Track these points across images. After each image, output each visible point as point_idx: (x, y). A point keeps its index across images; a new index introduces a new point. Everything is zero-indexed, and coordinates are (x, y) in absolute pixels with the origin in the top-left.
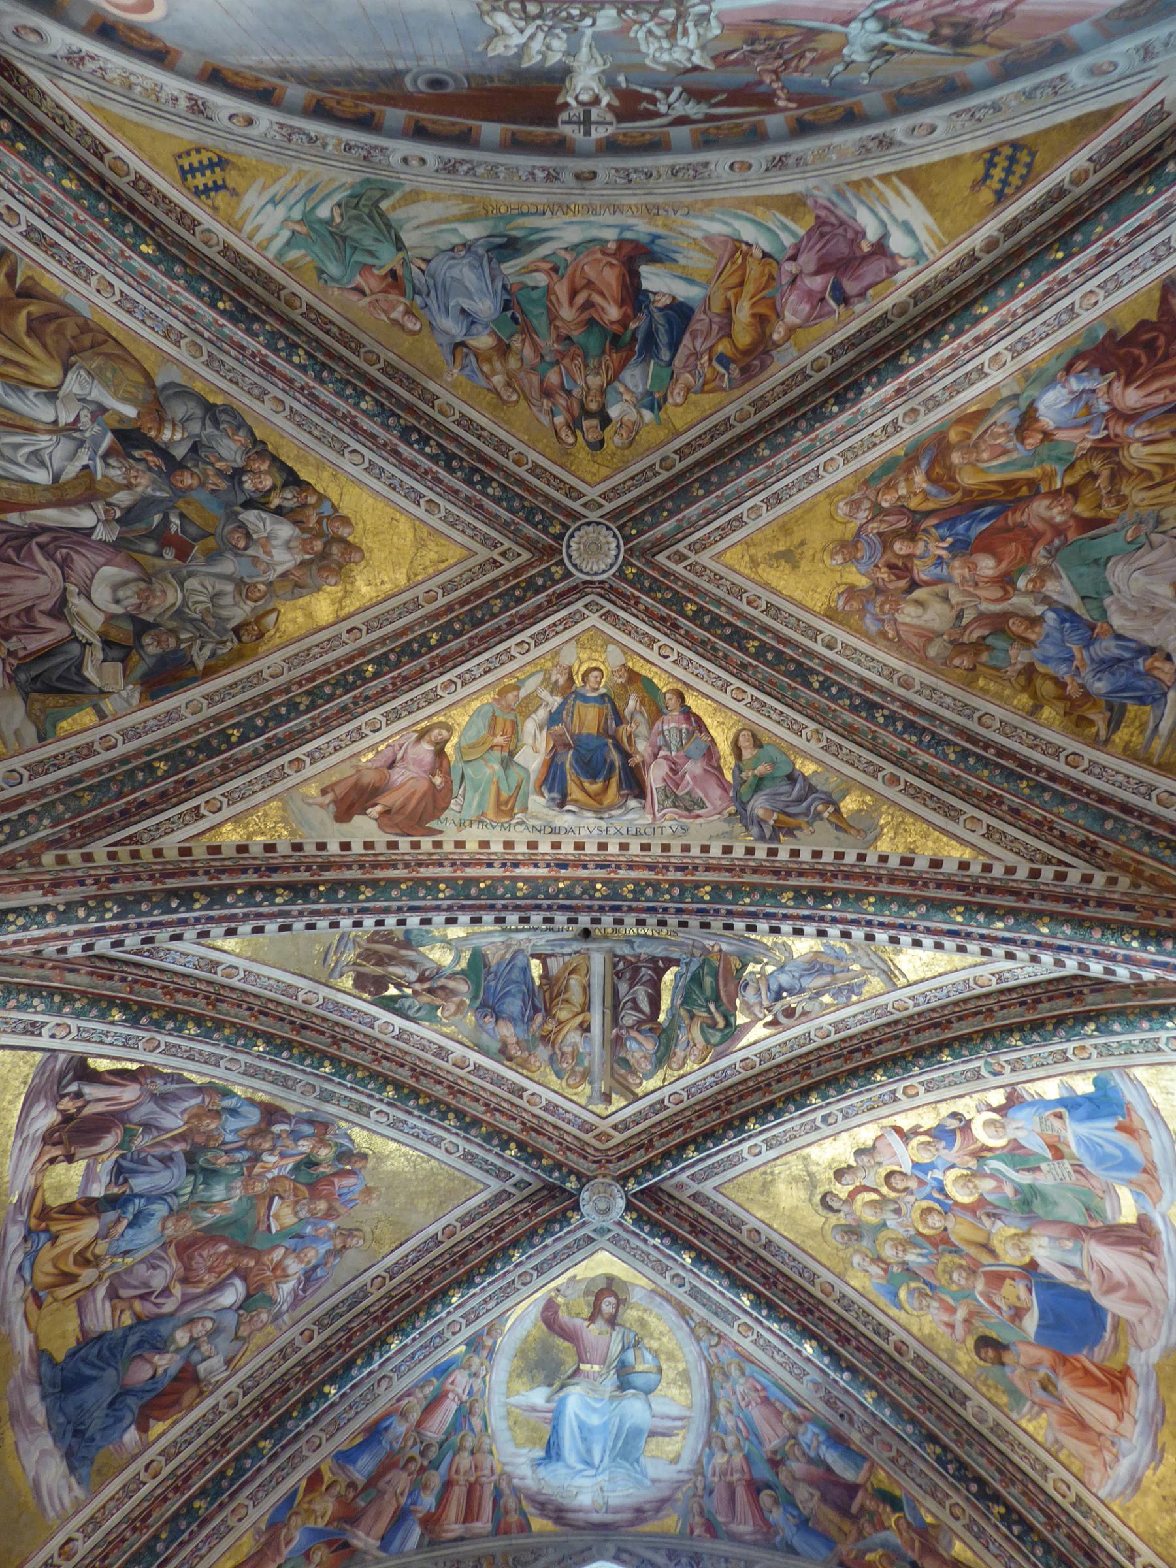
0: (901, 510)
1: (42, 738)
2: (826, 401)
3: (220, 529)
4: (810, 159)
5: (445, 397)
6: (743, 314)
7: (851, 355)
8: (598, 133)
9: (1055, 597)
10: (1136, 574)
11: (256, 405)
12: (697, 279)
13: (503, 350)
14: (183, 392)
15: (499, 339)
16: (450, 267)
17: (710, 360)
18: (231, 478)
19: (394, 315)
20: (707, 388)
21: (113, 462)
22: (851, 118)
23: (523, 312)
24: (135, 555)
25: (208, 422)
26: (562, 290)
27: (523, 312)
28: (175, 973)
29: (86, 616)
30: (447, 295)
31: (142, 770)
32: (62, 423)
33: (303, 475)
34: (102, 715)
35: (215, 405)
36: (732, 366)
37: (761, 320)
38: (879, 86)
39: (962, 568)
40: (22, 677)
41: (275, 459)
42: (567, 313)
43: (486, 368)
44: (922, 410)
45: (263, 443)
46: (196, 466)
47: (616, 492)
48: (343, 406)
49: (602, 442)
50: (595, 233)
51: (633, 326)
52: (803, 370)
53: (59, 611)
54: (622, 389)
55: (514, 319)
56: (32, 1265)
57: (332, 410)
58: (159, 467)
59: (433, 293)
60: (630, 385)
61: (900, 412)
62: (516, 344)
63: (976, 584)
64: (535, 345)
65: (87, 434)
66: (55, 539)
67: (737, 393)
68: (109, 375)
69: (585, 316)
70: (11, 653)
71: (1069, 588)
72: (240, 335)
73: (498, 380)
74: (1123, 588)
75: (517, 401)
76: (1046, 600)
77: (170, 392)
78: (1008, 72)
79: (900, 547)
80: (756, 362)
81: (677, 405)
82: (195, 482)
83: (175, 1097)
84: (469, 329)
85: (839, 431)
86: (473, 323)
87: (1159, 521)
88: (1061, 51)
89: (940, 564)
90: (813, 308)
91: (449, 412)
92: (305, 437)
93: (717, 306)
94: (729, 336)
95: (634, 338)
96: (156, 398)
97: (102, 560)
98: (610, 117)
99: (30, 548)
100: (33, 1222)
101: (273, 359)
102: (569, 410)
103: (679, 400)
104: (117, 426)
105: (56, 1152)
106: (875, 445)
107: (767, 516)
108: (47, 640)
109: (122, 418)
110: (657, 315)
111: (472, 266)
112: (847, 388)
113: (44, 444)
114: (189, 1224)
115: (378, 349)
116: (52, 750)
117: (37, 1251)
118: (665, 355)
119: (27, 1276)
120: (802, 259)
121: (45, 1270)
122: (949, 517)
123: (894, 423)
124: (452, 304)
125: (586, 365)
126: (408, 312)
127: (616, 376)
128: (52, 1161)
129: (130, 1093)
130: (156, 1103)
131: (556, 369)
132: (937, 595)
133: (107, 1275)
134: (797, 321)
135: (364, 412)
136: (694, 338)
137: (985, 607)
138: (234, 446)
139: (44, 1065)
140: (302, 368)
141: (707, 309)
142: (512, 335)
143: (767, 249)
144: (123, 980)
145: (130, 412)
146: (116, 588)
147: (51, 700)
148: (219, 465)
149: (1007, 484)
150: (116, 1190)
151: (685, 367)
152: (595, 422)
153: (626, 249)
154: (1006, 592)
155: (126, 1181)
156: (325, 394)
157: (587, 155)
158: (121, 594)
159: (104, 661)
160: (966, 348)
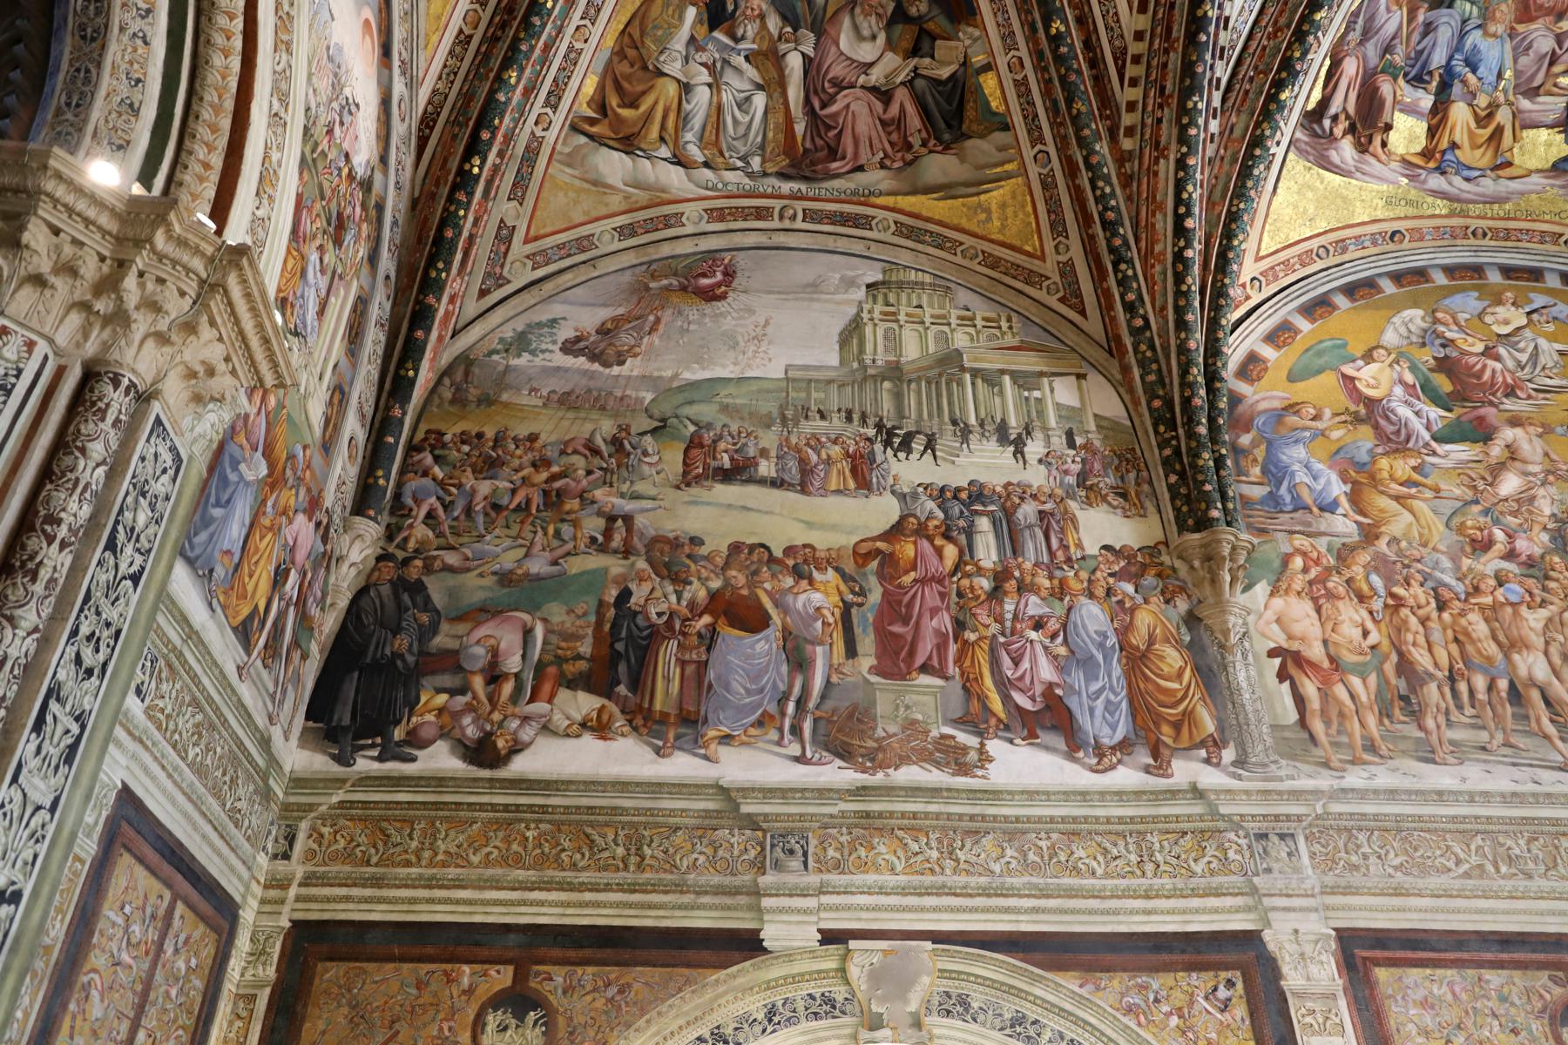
1: (1006, 127)
21: (740, 32)
24: (828, 15)
28: (1256, 22)
29: (888, 70)
31: (1058, 47)
32: (710, 80)
34: (988, 67)
40: (946, 136)
53: (884, 94)
56: (1470, 168)
65: (717, 56)
66: (816, 92)
68: (660, 33)
70: (924, 144)
83: (1371, 19)
97: (834, 49)
100: (1432, 165)
104: (706, 26)
105: (1377, 141)
108: (910, 109)
109: (698, 21)
114: (1504, 7)
116: (1018, 120)
117: (1459, 162)
119: (1477, 173)
121: (1482, 158)
128: (1384, 144)
129: (1350, 67)
130: (1368, 40)
133: (1511, 98)
139: (1300, 151)
144: (1251, 80)
145: (691, 13)
146: (860, 37)
147: (970, 113)
150: (1434, 84)
155: (1430, 73)
158: (866, 33)
159: (933, 57)
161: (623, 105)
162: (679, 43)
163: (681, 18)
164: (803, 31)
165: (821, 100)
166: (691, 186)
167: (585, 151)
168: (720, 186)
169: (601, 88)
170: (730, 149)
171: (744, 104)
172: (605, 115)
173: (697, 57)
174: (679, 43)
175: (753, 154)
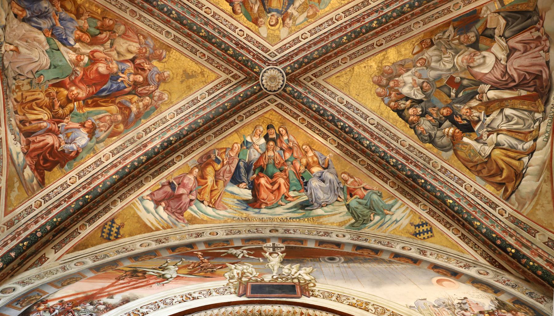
0: (141, 95)
2: (176, 142)
3: (434, 90)
4: (187, 236)
5: (333, 147)
6: (210, 179)
7: (166, 162)
8: (270, 244)
9: (71, 51)
10: (37, 59)
11: (412, 143)
12: (229, 193)
13: (308, 166)
14: (443, 148)
15: (309, 170)
16: (328, 198)
17: (223, 161)
18: (426, 113)
19: (352, 180)
20: (224, 150)
21: (476, 118)
22: (173, 248)
23: (299, 181)
25: (433, 136)
26: (283, 190)
27: (299, 181)
30: (330, 188)
32: (495, 134)
33: (396, 114)
35: (430, 143)
36: (214, 159)
37: (203, 176)
38: (163, 258)
39: (113, 68)
41: (407, 121)
42: (282, 181)
43: (315, 159)
44: (135, 138)
45: (411, 128)
46: (440, 118)
47: (262, 107)
48: (376, 142)
49: (268, 128)
50: (270, 211)
51: (255, 176)
52: (185, 156)
54: (259, 150)
55: (303, 179)
57: (381, 141)
58: (457, 117)
59: (336, 188)
60: (256, 152)
61: (145, 138)
62: (303, 168)
63: (106, 59)
64: (295, 168)
65: (485, 130)
67: (212, 148)
69: (274, 180)
71: (65, 55)
72: (416, 170)
73: (310, 154)
74: (41, 53)
75: (303, 145)
76: (75, 50)
77: (447, 148)
78: (115, 263)
79: (140, 79)
80: (205, 160)
81: (237, 143)
82: (442, 111)
84: (322, 175)
85: (169, 130)
86: (320, 177)
87: (30, 83)
88: (97, 269)
89: (122, 70)
90: (182, 181)
91: (331, 141)
92: (393, 130)
93: (221, 183)
94: (216, 171)
95: (254, 170)
96: (454, 145)
98: (265, 249)
99: (519, 80)
101: (404, 161)
102: (281, 142)
103: (236, 145)
104: (472, 134)
106: (154, 124)
107: (197, 94)
109: (469, 137)
110: (245, 180)
111: (319, 199)
112: (167, 147)
113: (505, 125)
115: (359, 166)
118: (241, 164)
120: (188, 200)
122: (120, 92)
123: (146, 133)
124: (328, 184)
125: (274, 160)
126: (346, 181)
127: (262, 155)
131: (286, 159)
132: (123, 55)
134: (188, 176)
135: (368, 140)
136: (230, 170)
137: (101, 49)
138: (424, 126)
140: (392, 157)
141: (225, 182)
142: (304, 172)
143: (202, 204)
145: (465, 140)
148: (431, 118)
149: (97, 105)
151: (233, 159)
152: (270, 137)
153: (258, 205)
154: (92, 55)
156: (383, 147)
157: (274, 237)
160: (120, 163)
161: (501, 175)
162: (478, 146)
163: (467, 144)
164: (479, 90)
165: (511, 82)
166: (545, 149)
167: (518, 196)
168: (547, 135)
169: (492, 183)
170: (529, 128)
171: (508, 119)
172: (504, 184)
173: (484, 139)
174: (478, 146)
175: (533, 116)
